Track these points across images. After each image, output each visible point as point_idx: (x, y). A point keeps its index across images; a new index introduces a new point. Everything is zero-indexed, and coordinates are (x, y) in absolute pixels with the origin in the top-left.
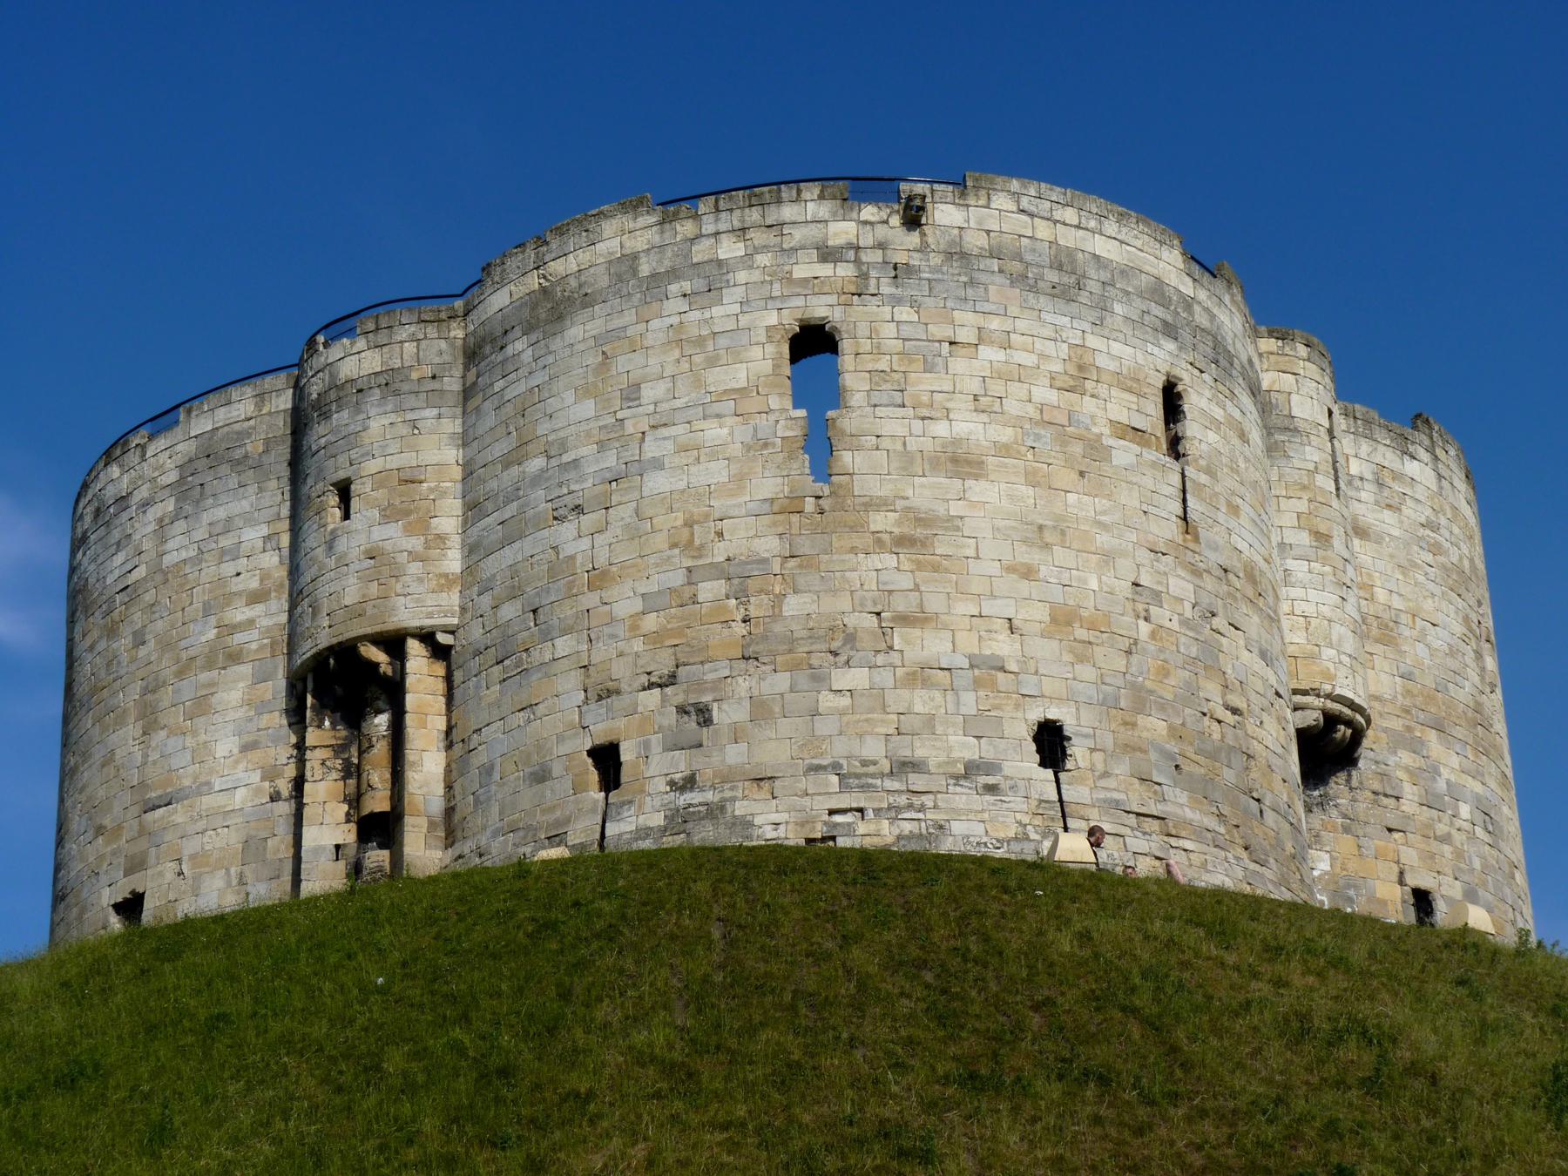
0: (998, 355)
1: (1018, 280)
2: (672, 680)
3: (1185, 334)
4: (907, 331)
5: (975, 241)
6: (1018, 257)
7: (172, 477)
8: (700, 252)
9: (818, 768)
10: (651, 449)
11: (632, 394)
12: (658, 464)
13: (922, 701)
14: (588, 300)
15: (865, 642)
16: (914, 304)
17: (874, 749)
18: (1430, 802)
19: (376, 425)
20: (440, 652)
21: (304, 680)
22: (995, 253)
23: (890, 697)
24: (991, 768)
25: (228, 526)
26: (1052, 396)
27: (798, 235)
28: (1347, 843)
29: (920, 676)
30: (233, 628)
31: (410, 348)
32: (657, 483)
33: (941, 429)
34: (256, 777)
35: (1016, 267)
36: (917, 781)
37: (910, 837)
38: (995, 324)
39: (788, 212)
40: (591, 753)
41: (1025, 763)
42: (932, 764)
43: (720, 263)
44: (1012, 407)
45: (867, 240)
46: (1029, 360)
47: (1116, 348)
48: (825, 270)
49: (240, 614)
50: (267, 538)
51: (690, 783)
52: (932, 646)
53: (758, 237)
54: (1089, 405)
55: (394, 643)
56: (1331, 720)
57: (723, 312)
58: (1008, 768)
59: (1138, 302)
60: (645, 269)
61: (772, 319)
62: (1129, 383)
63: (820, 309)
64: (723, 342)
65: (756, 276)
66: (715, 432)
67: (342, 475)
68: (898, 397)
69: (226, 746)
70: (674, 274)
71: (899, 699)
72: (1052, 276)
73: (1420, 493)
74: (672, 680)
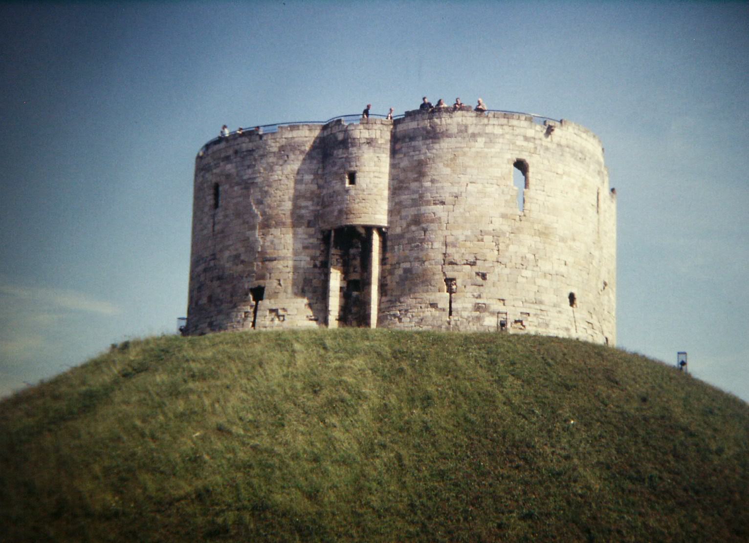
1: (573, 155)
6: (573, 149)
8: (489, 129)
9: (517, 299)
14: (449, 136)
19: (366, 156)
21: (330, 231)
23: (537, 280)
27: (518, 131)
30: (300, 208)
35: (572, 151)
48: (525, 144)
51: (479, 297)
55: (369, 229)
68: (542, 188)
71: (539, 281)
74: (473, 264)
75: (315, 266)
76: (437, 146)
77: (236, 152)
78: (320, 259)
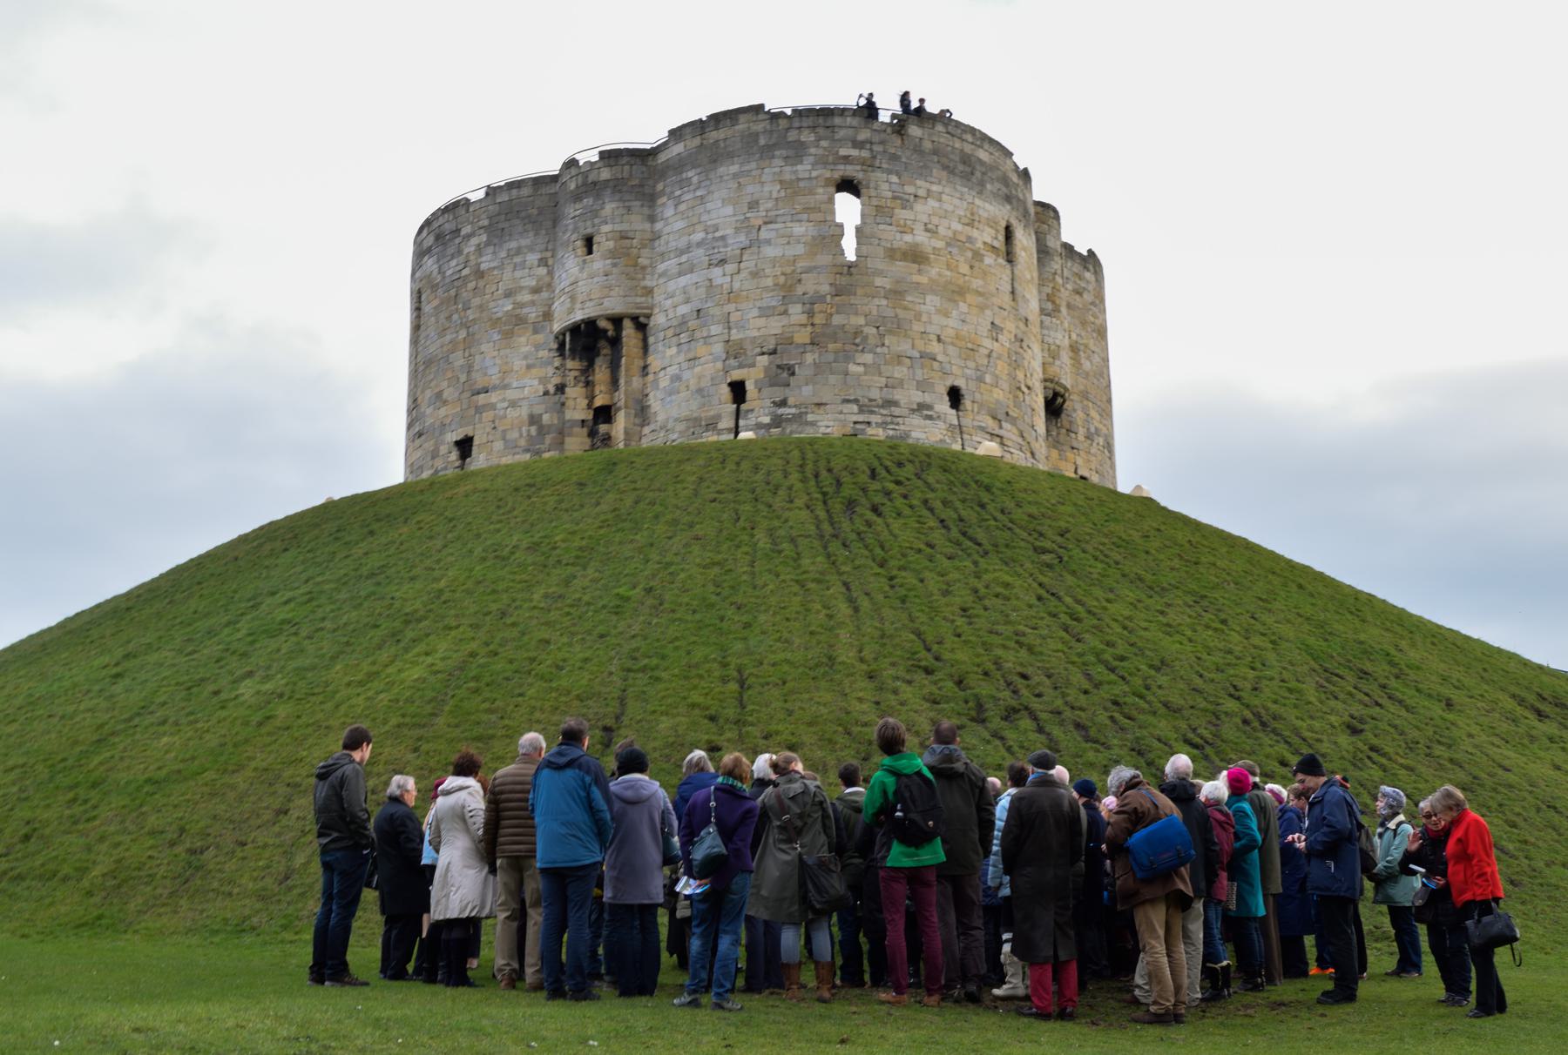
0: (937, 205)
1: (945, 167)
2: (774, 352)
4: (894, 187)
5: (927, 145)
7: (486, 223)
10: (764, 234)
11: (753, 205)
12: (768, 242)
13: (900, 372)
14: (731, 156)
15: (872, 341)
16: (898, 175)
17: (875, 394)
18: (1089, 437)
22: (935, 152)
24: (930, 407)
25: (519, 251)
26: (959, 227)
29: (899, 358)
30: (521, 305)
31: (627, 168)
32: (769, 252)
33: (908, 238)
34: (536, 382)
36: (896, 411)
37: (892, 437)
38: (935, 188)
39: (837, 120)
40: (731, 384)
41: (944, 406)
42: (902, 403)
43: (802, 143)
44: (942, 230)
45: (876, 138)
46: (950, 208)
47: (987, 205)
48: (854, 152)
49: (525, 297)
50: (541, 260)
51: (783, 403)
52: (904, 347)
53: (821, 131)
54: (975, 233)
55: (617, 321)
57: (803, 169)
58: (937, 407)
59: (998, 186)
60: (762, 142)
61: (828, 174)
62: (991, 222)
63: (851, 171)
64: (802, 184)
65: (820, 152)
66: (799, 229)
67: (589, 231)
72: (961, 167)
75: (546, 393)
76: (712, 175)
77: (438, 238)
78: (556, 380)
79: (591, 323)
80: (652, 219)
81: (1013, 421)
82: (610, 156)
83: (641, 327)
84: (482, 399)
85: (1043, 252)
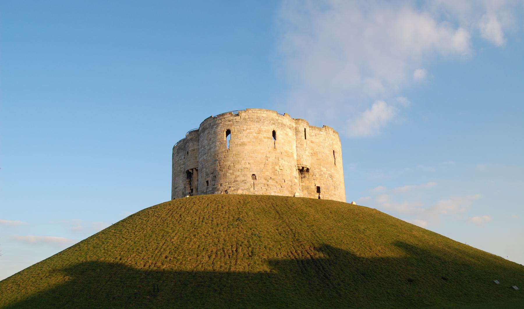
3: (277, 124)
5: (247, 117)
11: (210, 140)
14: (207, 129)
20: (197, 170)
24: (246, 180)
28: (307, 182)
33: (242, 141)
36: (237, 183)
38: (248, 127)
39: (225, 116)
41: (251, 180)
48: (229, 123)
49: (182, 166)
55: (192, 170)
56: (303, 168)
69: (181, 181)
70: (214, 125)
73: (322, 136)
79: (188, 171)
80: (198, 145)
81: (274, 179)
82: (191, 133)
83: (197, 170)
84: (176, 190)
85: (297, 131)
